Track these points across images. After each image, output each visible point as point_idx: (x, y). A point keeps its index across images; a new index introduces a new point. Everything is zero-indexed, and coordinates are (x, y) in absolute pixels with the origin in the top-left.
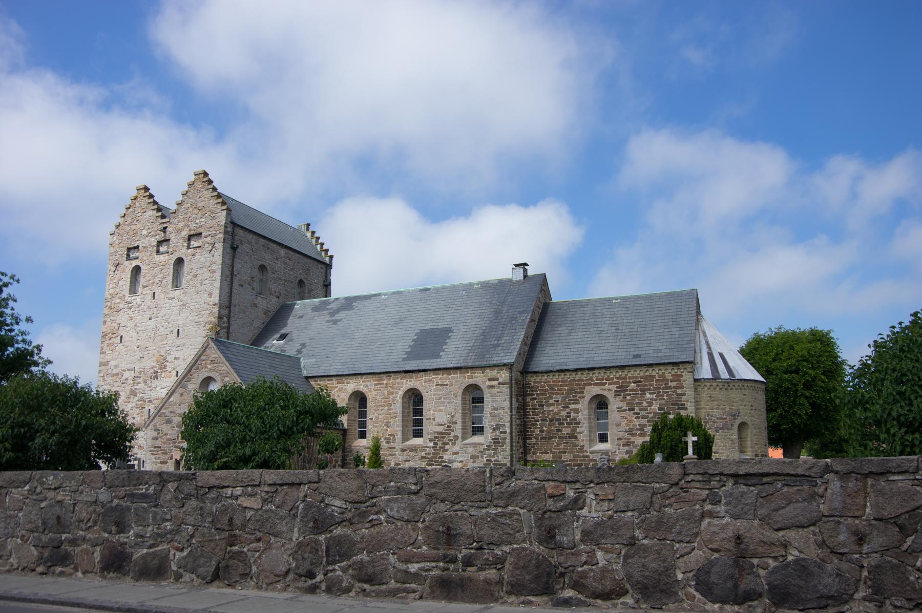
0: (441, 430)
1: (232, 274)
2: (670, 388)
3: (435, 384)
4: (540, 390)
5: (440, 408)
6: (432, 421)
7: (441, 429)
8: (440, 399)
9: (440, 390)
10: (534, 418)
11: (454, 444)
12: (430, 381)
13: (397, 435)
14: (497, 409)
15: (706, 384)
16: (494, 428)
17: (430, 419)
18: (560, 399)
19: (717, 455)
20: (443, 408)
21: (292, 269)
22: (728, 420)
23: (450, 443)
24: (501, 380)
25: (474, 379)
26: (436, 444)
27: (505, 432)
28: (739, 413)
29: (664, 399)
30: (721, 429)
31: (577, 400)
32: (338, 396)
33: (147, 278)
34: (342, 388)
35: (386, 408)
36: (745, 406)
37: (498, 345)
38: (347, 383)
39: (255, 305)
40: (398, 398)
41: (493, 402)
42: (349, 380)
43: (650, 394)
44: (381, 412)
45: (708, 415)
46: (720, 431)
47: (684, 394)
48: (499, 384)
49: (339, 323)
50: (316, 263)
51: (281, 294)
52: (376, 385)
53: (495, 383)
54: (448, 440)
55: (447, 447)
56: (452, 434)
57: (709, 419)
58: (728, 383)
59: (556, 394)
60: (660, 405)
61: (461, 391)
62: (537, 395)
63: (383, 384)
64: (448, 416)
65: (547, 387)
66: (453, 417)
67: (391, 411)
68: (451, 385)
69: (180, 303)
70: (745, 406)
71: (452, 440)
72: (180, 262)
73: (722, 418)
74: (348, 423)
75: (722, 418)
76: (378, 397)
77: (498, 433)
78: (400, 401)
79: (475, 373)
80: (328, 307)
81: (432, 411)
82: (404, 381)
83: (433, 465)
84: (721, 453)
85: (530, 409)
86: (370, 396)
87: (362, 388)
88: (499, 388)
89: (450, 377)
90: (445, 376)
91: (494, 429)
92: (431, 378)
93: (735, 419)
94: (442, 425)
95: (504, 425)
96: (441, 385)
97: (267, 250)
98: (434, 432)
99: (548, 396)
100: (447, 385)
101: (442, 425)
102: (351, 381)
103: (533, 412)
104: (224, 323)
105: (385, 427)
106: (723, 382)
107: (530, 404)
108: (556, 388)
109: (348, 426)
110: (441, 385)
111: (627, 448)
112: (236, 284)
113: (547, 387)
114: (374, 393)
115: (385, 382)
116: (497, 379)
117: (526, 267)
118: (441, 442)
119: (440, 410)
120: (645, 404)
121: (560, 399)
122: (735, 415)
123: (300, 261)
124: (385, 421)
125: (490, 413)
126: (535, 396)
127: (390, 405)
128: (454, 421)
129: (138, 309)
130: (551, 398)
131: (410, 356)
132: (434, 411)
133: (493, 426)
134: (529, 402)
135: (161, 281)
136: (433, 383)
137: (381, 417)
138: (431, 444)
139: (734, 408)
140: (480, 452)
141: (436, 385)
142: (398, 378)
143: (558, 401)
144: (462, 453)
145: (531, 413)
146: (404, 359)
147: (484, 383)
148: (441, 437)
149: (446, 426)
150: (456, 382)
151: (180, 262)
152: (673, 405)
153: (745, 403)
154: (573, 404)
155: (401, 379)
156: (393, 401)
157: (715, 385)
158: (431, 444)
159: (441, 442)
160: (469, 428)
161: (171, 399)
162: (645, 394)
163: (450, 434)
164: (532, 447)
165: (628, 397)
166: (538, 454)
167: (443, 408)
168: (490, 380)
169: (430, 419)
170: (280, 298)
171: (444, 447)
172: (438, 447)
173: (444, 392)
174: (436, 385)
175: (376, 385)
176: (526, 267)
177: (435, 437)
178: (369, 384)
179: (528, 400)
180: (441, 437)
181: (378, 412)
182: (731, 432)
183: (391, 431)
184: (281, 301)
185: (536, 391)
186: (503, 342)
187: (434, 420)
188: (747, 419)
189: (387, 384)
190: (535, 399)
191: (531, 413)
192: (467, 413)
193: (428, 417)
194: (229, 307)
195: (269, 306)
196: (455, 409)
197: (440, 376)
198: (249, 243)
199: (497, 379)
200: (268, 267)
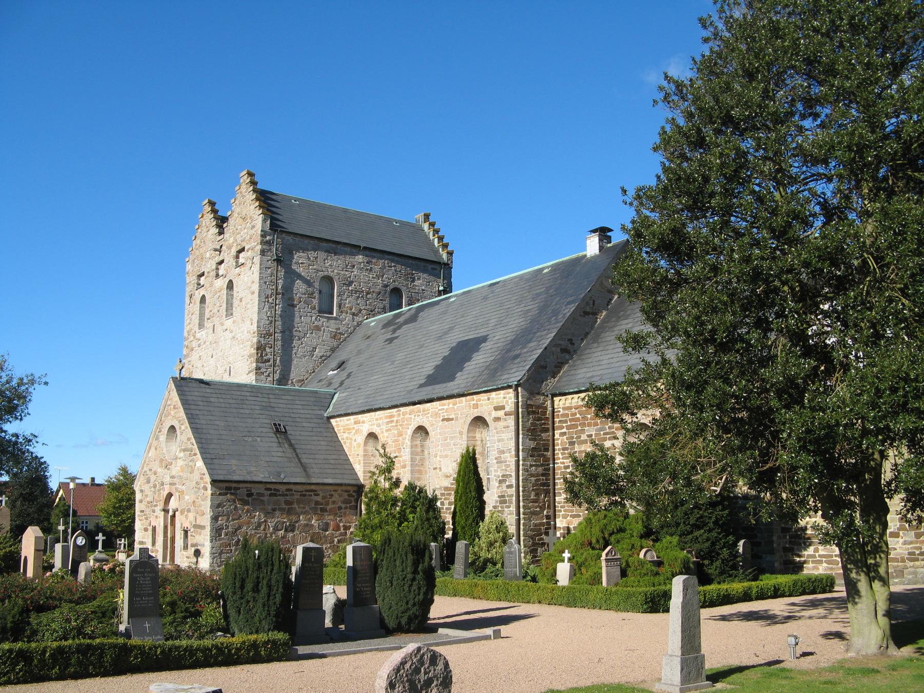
4: (571, 420)
5: (446, 453)
6: (438, 470)
10: (563, 463)
14: (503, 452)
16: (500, 480)
18: (593, 433)
24: (507, 409)
27: (510, 486)
31: (613, 433)
32: (355, 440)
33: (210, 309)
37: (517, 357)
38: (363, 422)
40: (407, 441)
41: (499, 441)
48: (506, 415)
49: (395, 341)
50: (422, 264)
51: (360, 310)
53: (501, 413)
59: (589, 425)
61: (467, 427)
62: (568, 428)
63: (392, 421)
65: (578, 416)
69: (231, 335)
72: (230, 285)
74: (364, 476)
77: (504, 485)
78: (409, 443)
79: (480, 400)
80: (397, 321)
82: (412, 416)
85: (559, 450)
88: (505, 420)
89: (455, 407)
90: (451, 406)
91: (500, 482)
92: (437, 410)
94: (447, 477)
95: (511, 476)
96: (448, 420)
99: (579, 428)
100: (452, 419)
101: (447, 477)
103: (562, 454)
107: (559, 442)
108: (589, 416)
109: (364, 480)
110: (448, 420)
113: (578, 416)
115: (395, 419)
116: (503, 408)
117: (609, 234)
119: (446, 456)
121: (593, 433)
125: (496, 459)
126: (564, 430)
129: (204, 346)
130: (583, 431)
131: (432, 380)
133: (499, 477)
134: (558, 439)
135: (218, 311)
141: (443, 420)
143: (591, 436)
145: (560, 456)
146: (421, 386)
147: (490, 414)
151: (230, 285)
154: (610, 439)
156: (403, 443)
161: (150, 455)
164: (561, 507)
166: (569, 518)
167: (449, 453)
168: (497, 408)
174: (443, 420)
175: (388, 423)
176: (609, 234)
178: (381, 422)
179: (557, 436)
185: (566, 422)
186: (525, 350)
187: (440, 469)
189: (397, 421)
190: (564, 434)
191: (560, 456)
193: (435, 466)
199: (503, 408)
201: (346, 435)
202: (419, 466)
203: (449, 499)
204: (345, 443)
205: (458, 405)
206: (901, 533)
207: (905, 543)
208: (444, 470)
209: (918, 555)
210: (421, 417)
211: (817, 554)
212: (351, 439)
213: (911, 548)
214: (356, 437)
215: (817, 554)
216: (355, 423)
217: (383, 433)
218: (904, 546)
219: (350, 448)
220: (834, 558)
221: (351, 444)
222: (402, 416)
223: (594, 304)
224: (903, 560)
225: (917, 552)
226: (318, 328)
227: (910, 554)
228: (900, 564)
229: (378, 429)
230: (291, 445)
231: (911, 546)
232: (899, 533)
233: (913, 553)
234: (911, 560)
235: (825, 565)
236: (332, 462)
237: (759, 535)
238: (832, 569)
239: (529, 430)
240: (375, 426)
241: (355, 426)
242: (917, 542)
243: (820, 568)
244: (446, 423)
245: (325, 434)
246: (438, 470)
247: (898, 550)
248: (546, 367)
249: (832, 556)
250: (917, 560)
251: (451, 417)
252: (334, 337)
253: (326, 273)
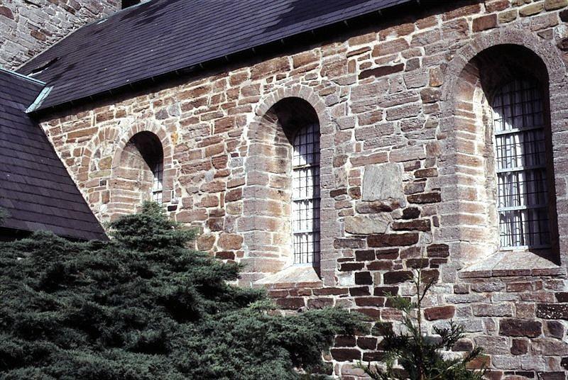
0: (379, 229)
3: (359, 72)
6: (348, 197)
7: (383, 225)
8: (375, 118)
9: (374, 90)
11: (431, 279)
12: (339, 66)
13: (240, 255)
17: (343, 192)
20: (388, 151)
23: (416, 273)
25: (504, 27)
26: (363, 279)
32: (98, 154)
34: (108, 130)
35: (214, 171)
40: (244, 135)
42: (122, 108)
44: (199, 185)
51: (78, 8)
52: (186, 107)
54: (409, 263)
55: (404, 289)
56: (424, 240)
63: (197, 104)
64: (406, 176)
66: (422, 176)
67: (225, 180)
68: (414, 65)
71: (420, 264)
76: (193, 144)
81: (348, 166)
83: (356, 355)
86: (173, 137)
87: (153, 125)
89: (408, 38)
92: (342, 57)
94: (387, 209)
96: (379, 72)
98: (358, 237)
100: (399, 68)
102: (127, 108)
105: (207, 231)
110: (379, 72)
114: (180, 131)
115: (209, 96)
118: (382, 273)
119: (379, 159)
124: (208, 210)
127: (221, 162)
128: (427, 190)
132: (355, 162)
136: (353, 71)
137: (197, 199)
138: (348, 281)
140: (543, 307)
142: (244, 77)
144: (465, 313)
147: (545, 32)
148: (381, 254)
149: (400, 211)
150: (430, 51)
155: (254, 78)
156: (232, 144)
158: (348, 281)
159: (382, 273)
160: (485, 217)
163: (415, 239)
169: (343, 192)
170: (76, 13)
171: (395, 291)
172: (371, 289)
173: (386, 94)
175: (186, 107)
177: (361, 255)
178: (168, 108)
180: (381, 254)
181: (190, 186)
183: (221, 243)
184: (78, 20)
187: (356, 193)
189: (215, 99)
192: (475, 162)
193: (337, 186)
195: (47, 22)
196: (432, 149)
197: (372, 45)
201: (72, 148)
202: (273, 196)
203: (388, 265)
204: (71, 162)
205: (417, 31)
208: (371, 193)
210: (289, 79)
212: (88, 152)
214: (101, 146)
216: (99, 119)
217: (173, 128)
219: (83, 173)
221: (86, 161)
222: (228, 87)
229: (158, 122)
236: (45, 192)
240: (154, 117)
241: (99, 125)
244: (375, 80)
245: (27, 142)
246: (348, 197)
251: (392, 64)
252: (35, 34)
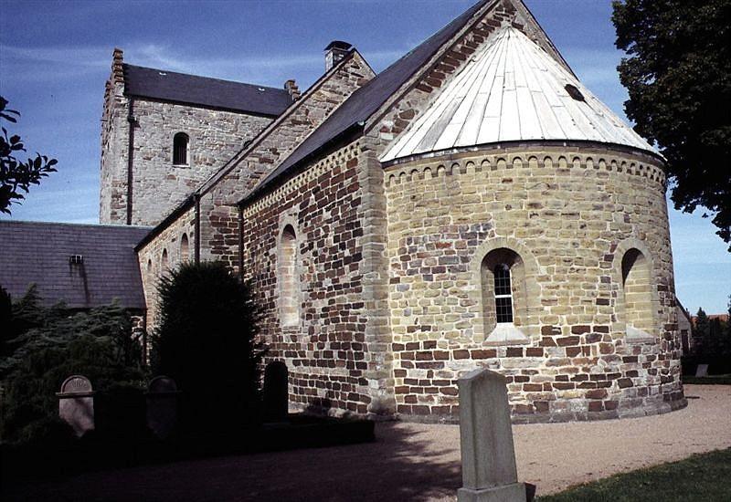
1: (131, 148)
2: (343, 193)
15: (403, 169)
19: (427, 333)
21: (232, 132)
22: (453, 248)
28: (487, 227)
29: (338, 218)
30: (435, 271)
36: (508, 207)
39: (173, 177)
43: (328, 210)
45: (410, 240)
46: (435, 276)
47: (358, 202)
57: (413, 250)
58: (451, 158)
60: (337, 230)
70: (508, 207)
73: (438, 246)
75: (438, 246)
84: (435, 330)
93: (474, 243)
97: (189, 116)
104: (123, 201)
106: (440, 158)
111: (308, 323)
112: (137, 159)
120: (322, 233)
122: (474, 234)
123: (247, 120)
139: (470, 216)
152: (350, 226)
153: (507, 201)
157: (420, 167)
162: (321, 212)
165: (309, 222)
182: (462, 275)
188: (514, 242)
194: (129, 184)
198: (158, 111)
200: (190, 134)
206: (545, 349)
207: (551, 363)
209: (572, 379)
211: (431, 379)
213: (561, 370)
215: (431, 379)
218: (550, 368)
220: (451, 386)
223: (307, 114)
224: (548, 388)
225: (571, 376)
226: (173, 177)
227: (558, 378)
228: (543, 393)
230: (84, 275)
231: (562, 367)
232: (542, 350)
233: (565, 378)
234: (560, 387)
235: (441, 394)
237: (365, 353)
238: (447, 400)
239: (211, 243)
242: (569, 363)
243: (435, 398)
247: (541, 374)
248: (238, 178)
249: (448, 383)
250: (571, 387)
253: (181, 131)
